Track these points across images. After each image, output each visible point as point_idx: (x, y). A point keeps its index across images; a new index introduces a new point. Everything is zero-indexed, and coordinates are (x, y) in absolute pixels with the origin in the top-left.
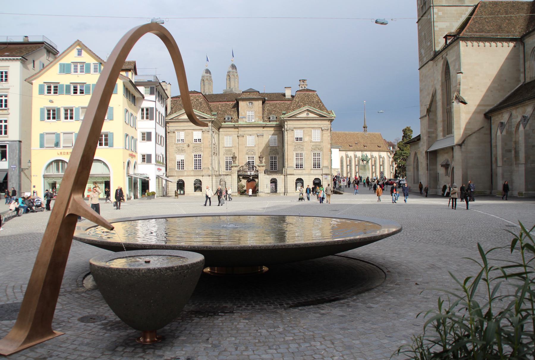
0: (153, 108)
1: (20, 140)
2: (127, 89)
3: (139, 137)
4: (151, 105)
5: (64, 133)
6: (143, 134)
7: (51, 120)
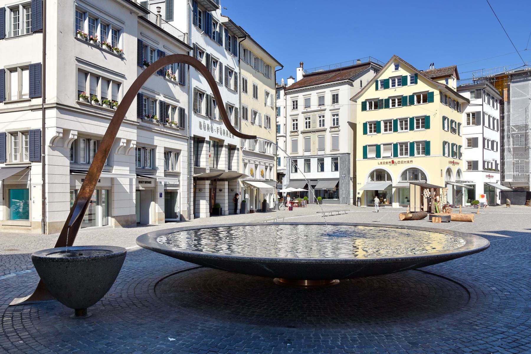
0: (480, 112)
1: (349, 152)
2: (446, 96)
3: (464, 143)
4: (479, 109)
5: (384, 145)
6: (469, 140)
7: (388, 132)
